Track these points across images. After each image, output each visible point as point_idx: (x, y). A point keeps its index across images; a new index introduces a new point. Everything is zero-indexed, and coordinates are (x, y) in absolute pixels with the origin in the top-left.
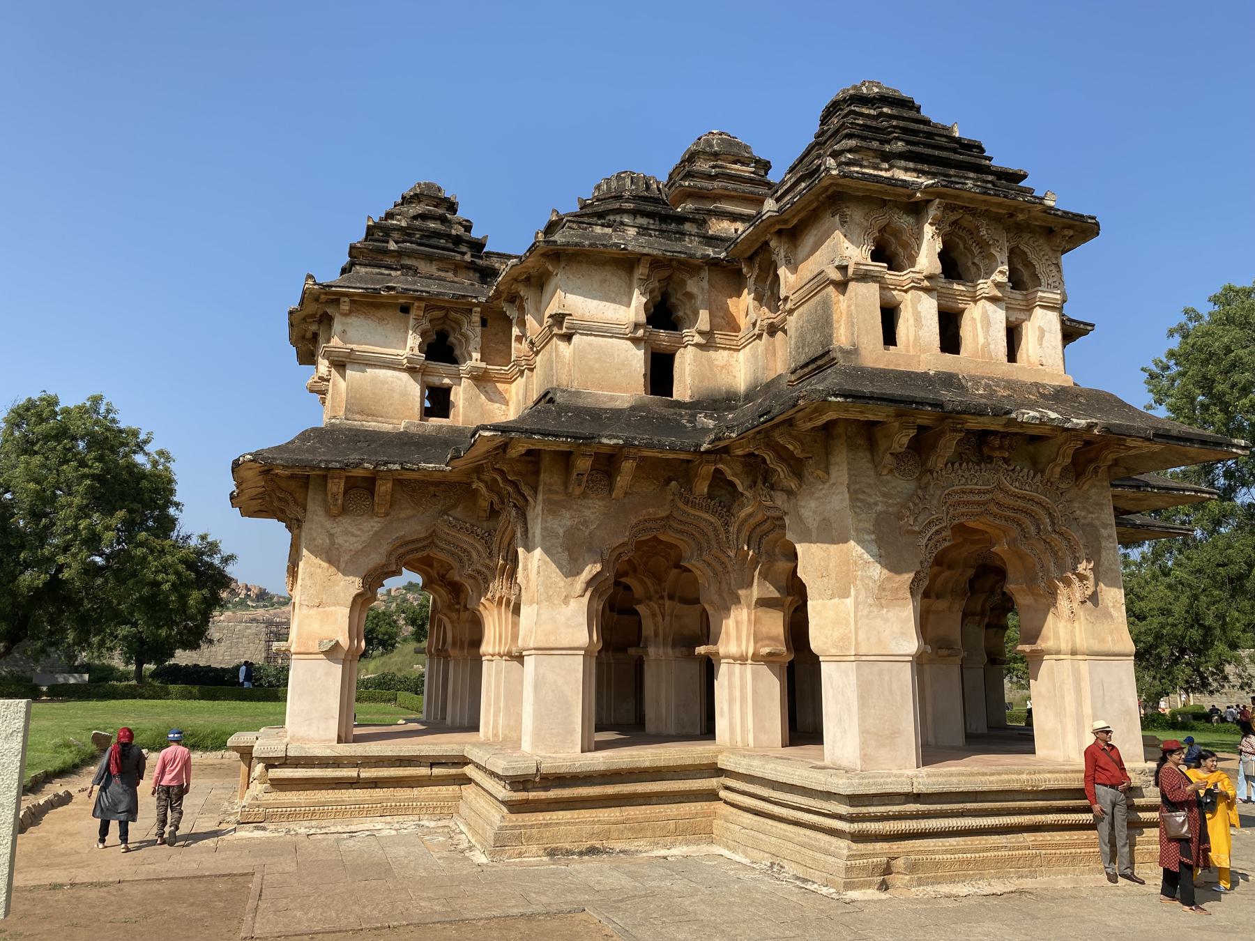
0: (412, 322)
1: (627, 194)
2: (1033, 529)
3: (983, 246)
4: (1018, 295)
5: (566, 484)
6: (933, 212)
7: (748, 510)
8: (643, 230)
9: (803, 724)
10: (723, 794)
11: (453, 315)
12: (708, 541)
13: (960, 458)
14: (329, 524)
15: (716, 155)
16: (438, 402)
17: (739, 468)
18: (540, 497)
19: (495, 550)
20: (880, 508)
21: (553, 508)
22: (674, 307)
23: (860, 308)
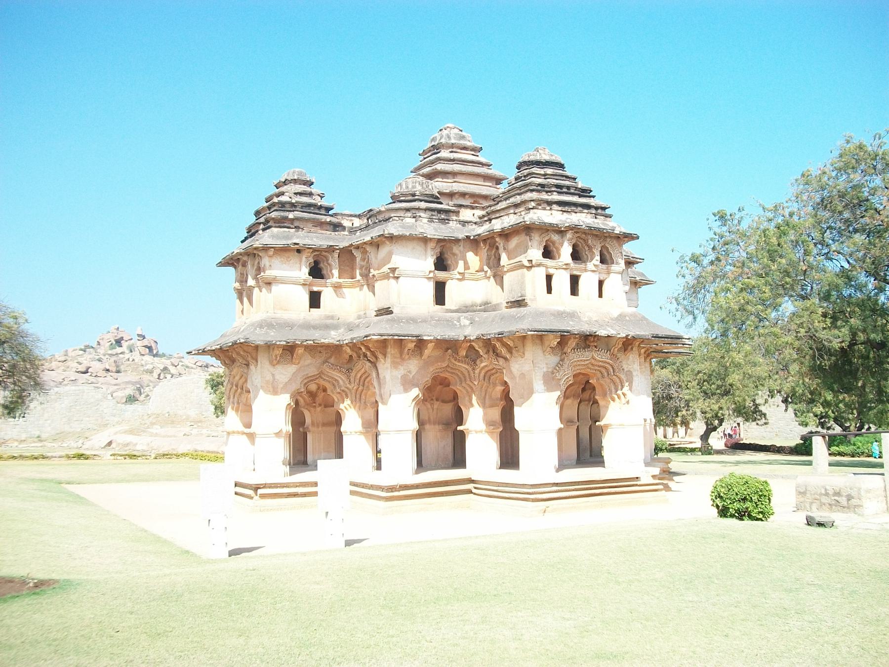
0: (304, 259)
1: (418, 193)
2: (606, 374)
3: (590, 248)
4: (604, 266)
5: (401, 353)
6: (569, 235)
7: (483, 364)
8: (431, 220)
9: (509, 458)
10: (474, 491)
11: (324, 253)
12: (465, 377)
13: (577, 347)
14: (272, 369)
15: (453, 146)
16: (315, 300)
17: (481, 344)
18: (389, 360)
19: (352, 380)
20: (545, 370)
21: (395, 365)
22: (447, 259)
23: (543, 292)
